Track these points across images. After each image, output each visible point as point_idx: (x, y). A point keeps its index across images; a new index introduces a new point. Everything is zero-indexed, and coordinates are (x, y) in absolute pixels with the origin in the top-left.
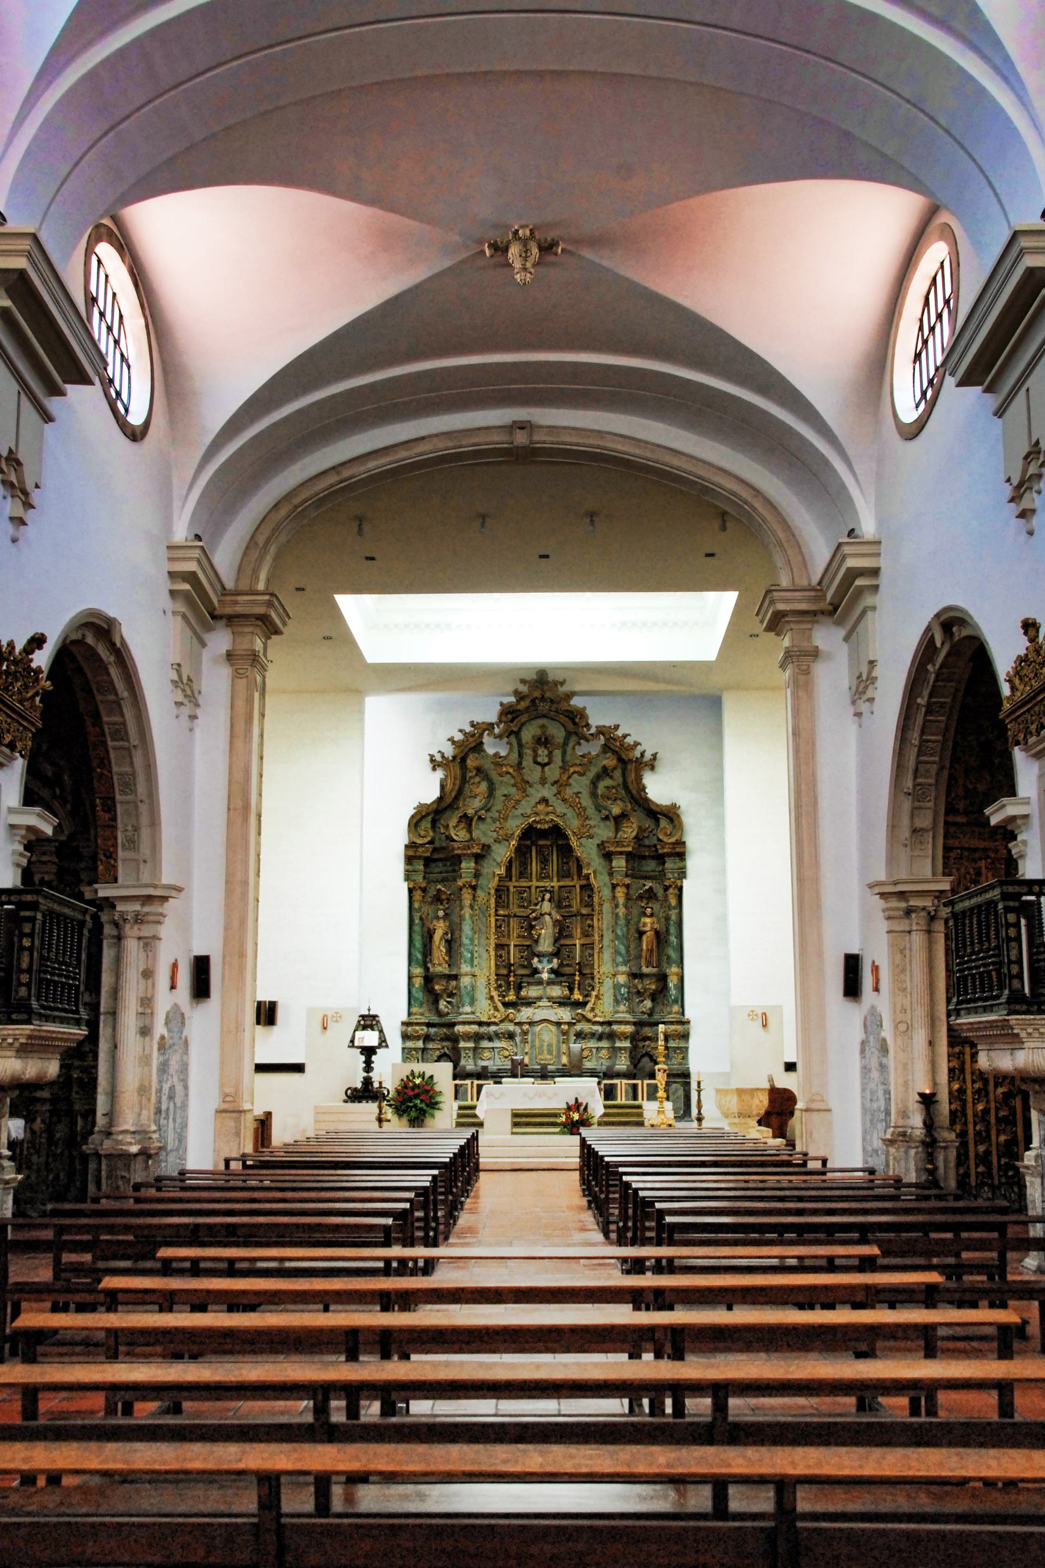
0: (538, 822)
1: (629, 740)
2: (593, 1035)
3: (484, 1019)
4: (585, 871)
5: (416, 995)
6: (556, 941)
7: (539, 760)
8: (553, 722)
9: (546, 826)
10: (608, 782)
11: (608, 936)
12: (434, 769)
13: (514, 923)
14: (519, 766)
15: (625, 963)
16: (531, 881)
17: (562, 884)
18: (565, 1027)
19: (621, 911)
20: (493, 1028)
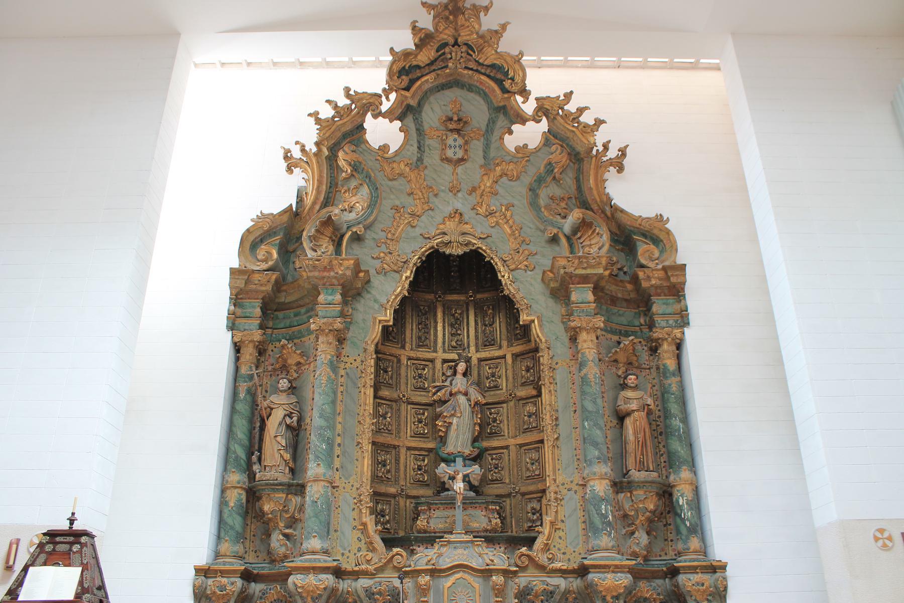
0: (447, 244)
1: (587, 118)
3: (348, 566)
4: (524, 318)
5: (230, 521)
6: (475, 440)
7: (450, 153)
9: (460, 252)
10: (553, 190)
11: (567, 421)
12: (289, 170)
13: (407, 411)
16: (435, 351)
17: (483, 355)
18: (498, 579)
19: (592, 371)
20: (364, 582)
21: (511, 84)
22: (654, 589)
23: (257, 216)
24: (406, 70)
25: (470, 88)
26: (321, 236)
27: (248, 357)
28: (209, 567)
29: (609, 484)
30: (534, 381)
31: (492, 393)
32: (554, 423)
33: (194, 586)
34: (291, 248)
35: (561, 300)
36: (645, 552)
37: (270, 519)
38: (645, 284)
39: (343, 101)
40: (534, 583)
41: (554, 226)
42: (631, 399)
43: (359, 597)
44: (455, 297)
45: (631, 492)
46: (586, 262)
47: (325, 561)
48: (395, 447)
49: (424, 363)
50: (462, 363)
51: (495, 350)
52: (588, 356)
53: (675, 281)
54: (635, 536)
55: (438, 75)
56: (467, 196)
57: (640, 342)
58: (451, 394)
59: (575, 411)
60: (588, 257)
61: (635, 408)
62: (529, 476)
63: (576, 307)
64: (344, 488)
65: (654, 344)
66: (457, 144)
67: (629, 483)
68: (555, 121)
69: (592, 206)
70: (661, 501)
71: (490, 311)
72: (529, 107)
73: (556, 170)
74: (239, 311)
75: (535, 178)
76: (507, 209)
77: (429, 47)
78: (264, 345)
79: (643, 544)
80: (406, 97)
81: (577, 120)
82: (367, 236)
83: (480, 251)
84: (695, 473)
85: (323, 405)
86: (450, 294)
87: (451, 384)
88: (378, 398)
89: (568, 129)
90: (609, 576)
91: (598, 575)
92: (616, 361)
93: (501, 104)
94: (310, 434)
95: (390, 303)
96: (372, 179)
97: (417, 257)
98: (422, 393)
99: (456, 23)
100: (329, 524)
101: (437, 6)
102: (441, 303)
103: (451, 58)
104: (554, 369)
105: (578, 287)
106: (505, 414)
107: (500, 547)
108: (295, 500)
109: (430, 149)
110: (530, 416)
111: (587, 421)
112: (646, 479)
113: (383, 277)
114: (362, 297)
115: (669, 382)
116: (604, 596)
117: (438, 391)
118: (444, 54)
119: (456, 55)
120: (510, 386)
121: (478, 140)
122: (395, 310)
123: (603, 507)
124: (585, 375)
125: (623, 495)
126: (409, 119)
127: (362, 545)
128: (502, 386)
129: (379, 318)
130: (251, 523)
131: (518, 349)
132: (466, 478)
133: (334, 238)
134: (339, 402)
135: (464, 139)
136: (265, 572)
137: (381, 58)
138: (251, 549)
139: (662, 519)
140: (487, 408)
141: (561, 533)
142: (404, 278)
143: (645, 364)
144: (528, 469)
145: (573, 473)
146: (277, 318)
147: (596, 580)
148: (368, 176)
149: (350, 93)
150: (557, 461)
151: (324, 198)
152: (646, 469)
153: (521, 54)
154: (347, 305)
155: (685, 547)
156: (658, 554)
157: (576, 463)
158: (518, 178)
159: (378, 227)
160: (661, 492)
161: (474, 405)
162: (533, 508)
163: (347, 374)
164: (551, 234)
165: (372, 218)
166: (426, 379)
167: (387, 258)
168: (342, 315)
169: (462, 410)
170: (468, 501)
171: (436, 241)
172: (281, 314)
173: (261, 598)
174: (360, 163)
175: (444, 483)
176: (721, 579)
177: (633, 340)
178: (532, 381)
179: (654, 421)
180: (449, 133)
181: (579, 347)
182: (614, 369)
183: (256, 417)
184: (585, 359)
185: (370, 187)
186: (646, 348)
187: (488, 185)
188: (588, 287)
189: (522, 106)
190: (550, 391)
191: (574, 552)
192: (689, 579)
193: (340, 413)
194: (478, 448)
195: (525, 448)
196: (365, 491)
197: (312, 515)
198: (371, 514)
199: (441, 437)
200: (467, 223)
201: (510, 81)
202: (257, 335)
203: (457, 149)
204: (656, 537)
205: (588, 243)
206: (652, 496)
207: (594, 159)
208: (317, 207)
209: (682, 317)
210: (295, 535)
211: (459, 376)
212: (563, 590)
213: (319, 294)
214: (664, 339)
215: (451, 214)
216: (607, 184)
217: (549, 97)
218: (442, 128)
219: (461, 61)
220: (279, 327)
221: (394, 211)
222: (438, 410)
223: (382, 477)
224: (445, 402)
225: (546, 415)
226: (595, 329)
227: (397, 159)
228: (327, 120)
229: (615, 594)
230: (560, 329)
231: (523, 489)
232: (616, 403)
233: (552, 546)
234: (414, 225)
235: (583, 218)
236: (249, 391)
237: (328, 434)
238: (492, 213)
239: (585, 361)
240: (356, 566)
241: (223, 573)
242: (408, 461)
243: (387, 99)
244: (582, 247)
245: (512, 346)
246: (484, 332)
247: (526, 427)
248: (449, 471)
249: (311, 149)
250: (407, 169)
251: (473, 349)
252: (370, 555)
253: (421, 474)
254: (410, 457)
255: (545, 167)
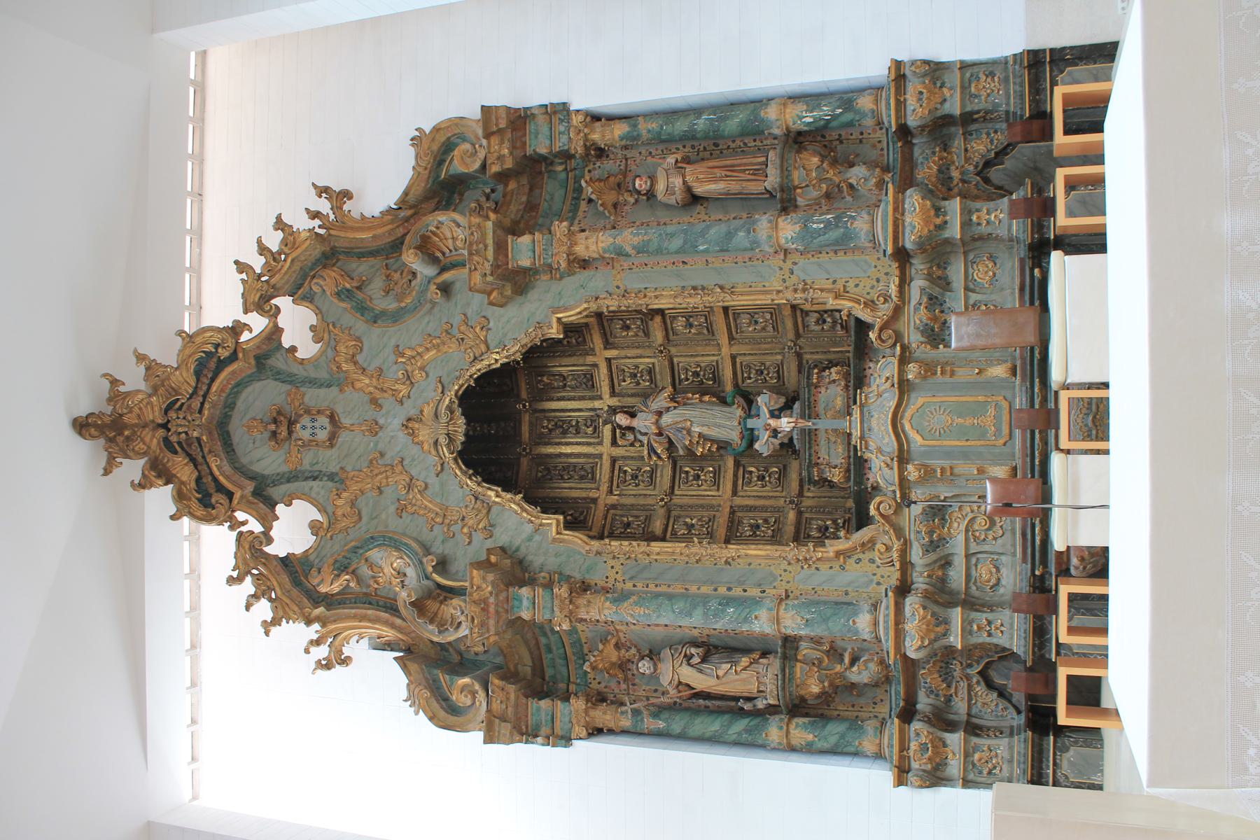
0: (451, 440)
1: (274, 241)
2: (934, 302)
3: (894, 576)
4: (555, 332)
5: (833, 740)
6: (723, 401)
7: (322, 435)
8: (240, 404)
10: (376, 287)
11: (698, 274)
12: (345, 661)
14: (337, 479)
15: (750, 228)
16: (600, 456)
17: (605, 389)
18: (912, 372)
19: (628, 238)
20: (916, 555)
21: (224, 347)
22: (927, 159)
23: (410, 706)
24: (204, 496)
25: (230, 406)
26: (439, 616)
27: (608, 717)
28: (896, 767)
29: (784, 218)
30: (642, 319)
31: (658, 377)
32: (700, 292)
33: (921, 787)
34: (455, 658)
35: (530, 280)
36: (878, 170)
37: (831, 684)
38: (509, 164)
39: (248, 586)
40: (918, 322)
41: (426, 290)
42: (668, 184)
43: (935, 562)
44: (525, 429)
45: (796, 188)
46: (477, 246)
47: (887, 608)
48: (732, 512)
49: (616, 472)
50: (617, 419)
51: (598, 372)
52: (608, 243)
53: (505, 121)
54: (855, 183)
55: (210, 452)
56: (384, 411)
57: (589, 171)
58: (660, 434)
59: (683, 262)
60: (470, 242)
61: (681, 180)
62: (773, 327)
63: (540, 260)
64: (788, 582)
65: (592, 152)
66: (309, 425)
67: (782, 190)
68: (278, 286)
69: (399, 235)
70: (808, 147)
71: (545, 379)
72: (258, 323)
73: (348, 286)
74: (545, 730)
75: (358, 315)
76: (402, 355)
77: (170, 464)
78: (592, 694)
79: (865, 172)
80: (242, 497)
81: (277, 256)
82: (439, 551)
83: (461, 392)
84: (770, 99)
85: (674, 612)
86: (520, 434)
87: (646, 434)
88: (665, 536)
89: (290, 267)
90: (908, 219)
91: (907, 234)
92: (615, 206)
93: (253, 362)
94: (715, 629)
95: (533, 519)
96: (359, 545)
97: (469, 482)
98: (658, 475)
99: (136, 425)
100: (837, 603)
101: (110, 453)
102: (533, 449)
103: (186, 433)
104: (625, 291)
105: (513, 256)
106: (688, 359)
107: (870, 368)
108: (805, 650)
109: (317, 463)
110: (691, 326)
111: (697, 247)
112: (778, 167)
113: (497, 529)
114: (524, 558)
115: (644, 132)
116: (936, 226)
117: (655, 453)
118: (179, 443)
119: (181, 426)
120: (648, 352)
121: (304, 394)
122: (543, 512)
123: (815, 226)
124: (634, 248)
125: (799, 199)
126: (274, 492)
127: (868, 555)
128: (648, 363)
129: (554, 534)
130: (836, 710)
131: (598, 341)
132: (775, 414)
133: (441, 598)
134: (670, 590)
135: (302, 415)
136: (902, 689)
137: (186, 532)
138: (871, 709)
139: (833, 146)
140: (680, 384)
141: (851, 284)
142: (497, 500)
143: (620, 165)
144: (764, 329)
145: (769, 266)
146: (553, 677)
147: (913, 237)
148: (355, 550)
149: (235, 576)
150: (752, 289)
151: (386, 612)
152: (764, 167)
153: (181, 333)
154: (535, 579)
155: (870, 115)
156: (880, 153)
157: (755, 263)
158: (358, 339)
159: (426, 536)
160: (796, 146)
161: (675, 402)
162: (817, 323)
163: (631, 578)
164: (437, 294)
165: (414, 545)
166: (639, 469)
167: (471, 522)
168: (549, 586)
169: (682, 419)
170: (807, 412)
171: (447, 455)
172: (549, 672)
173: (937, 695)
174: (336, 561)
175: (782, 445)
176: (913, 68)
177: (586, 182)
178: (642, 322)
179: (698, 155)
180: (294, 436)
181: (595, 256)
182: (626, 208)
183: (692, 705)
184: (611, 248)
185: (370, 547)
186: (598, 164)
187: (367, 381)
188: (512, 241)
189: (255, 333)
190: (656, 297)
191: (876, 267)
192: (914, 110)
193: (686, 589)
194: (734, 397)
195: (734, 333)
196: (792, 554)
197: (824, 627)
198: (823, 545)
199: (718, 449)
200: (422, 411)
201: (220, 350)
202: (578, 704)
203: (316, 424)
204: (857, 155)
205: (450, 241)
206: (800, 159)
207: (332, 232)
208: (398, 621)
209: (555, 113)
210: (853, 649)
211: (635, 423)
212: (928, 283)
213: (520, 618)
214: (586, 140)
215: (408, 434)
216: (368, 214)
217: (243, 294)
218: (286, 446)
219: (190, 418)
220: (566, 674)
221: (404, 514)
222: (681, 452)
223: (773, 530)
224: (670, 442)
225: (688, 303)
226: (571, 234)
227: (330, 510)
228: (275, 609)
229: (932, 212)
230: (570, 283)
231: (791, 335)
232: (674, 206)
233: (868, 297)
234: (423, 485)
235: (415, 248)
236: (655, 715)
237: (714, 604)
238: (408, 375)
239: (614, 248)
240: (893, 565)
241: (903, 747)
242: (753, 494)
243: (244, 523)
244: (456, 250)
245: (593, 350)
246: (573, 388)
247: (705, 331)
248: (766, 437)
249: (317, 631)
250: (345, 495)
251: (597, 404)
252: (879, 546)
253: (770, 476)
254: (746, 491)
255: (343, 300)
